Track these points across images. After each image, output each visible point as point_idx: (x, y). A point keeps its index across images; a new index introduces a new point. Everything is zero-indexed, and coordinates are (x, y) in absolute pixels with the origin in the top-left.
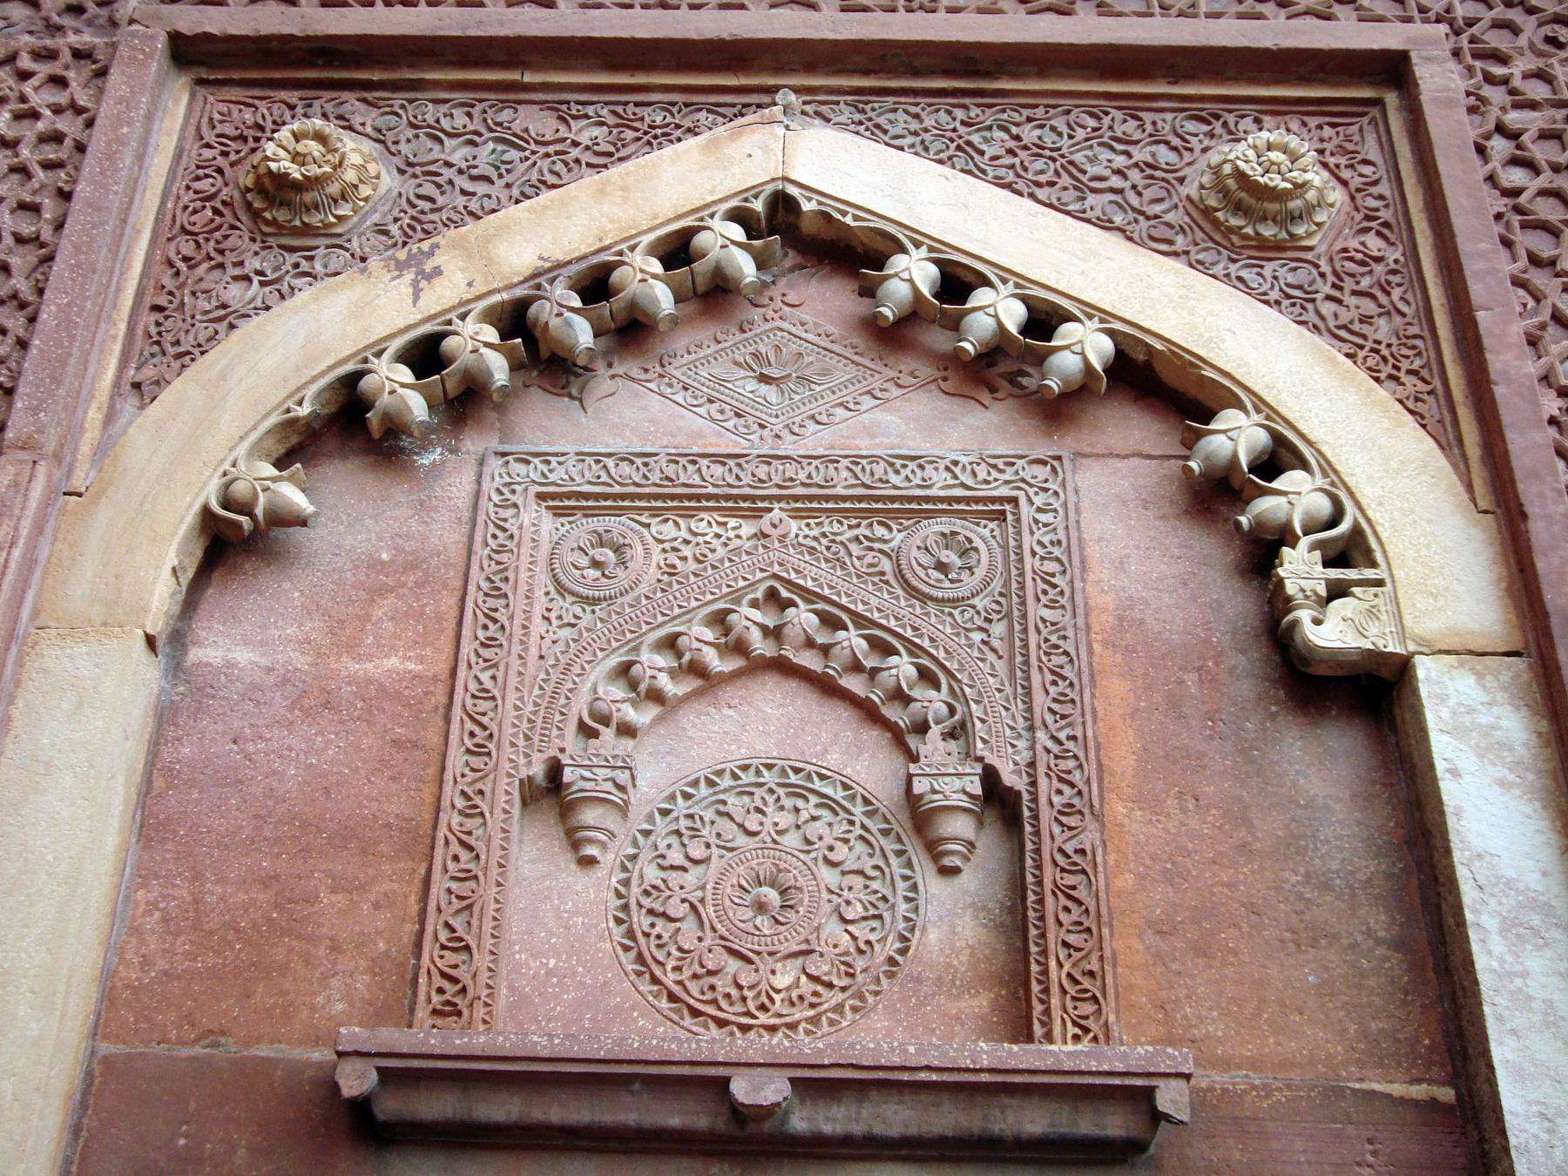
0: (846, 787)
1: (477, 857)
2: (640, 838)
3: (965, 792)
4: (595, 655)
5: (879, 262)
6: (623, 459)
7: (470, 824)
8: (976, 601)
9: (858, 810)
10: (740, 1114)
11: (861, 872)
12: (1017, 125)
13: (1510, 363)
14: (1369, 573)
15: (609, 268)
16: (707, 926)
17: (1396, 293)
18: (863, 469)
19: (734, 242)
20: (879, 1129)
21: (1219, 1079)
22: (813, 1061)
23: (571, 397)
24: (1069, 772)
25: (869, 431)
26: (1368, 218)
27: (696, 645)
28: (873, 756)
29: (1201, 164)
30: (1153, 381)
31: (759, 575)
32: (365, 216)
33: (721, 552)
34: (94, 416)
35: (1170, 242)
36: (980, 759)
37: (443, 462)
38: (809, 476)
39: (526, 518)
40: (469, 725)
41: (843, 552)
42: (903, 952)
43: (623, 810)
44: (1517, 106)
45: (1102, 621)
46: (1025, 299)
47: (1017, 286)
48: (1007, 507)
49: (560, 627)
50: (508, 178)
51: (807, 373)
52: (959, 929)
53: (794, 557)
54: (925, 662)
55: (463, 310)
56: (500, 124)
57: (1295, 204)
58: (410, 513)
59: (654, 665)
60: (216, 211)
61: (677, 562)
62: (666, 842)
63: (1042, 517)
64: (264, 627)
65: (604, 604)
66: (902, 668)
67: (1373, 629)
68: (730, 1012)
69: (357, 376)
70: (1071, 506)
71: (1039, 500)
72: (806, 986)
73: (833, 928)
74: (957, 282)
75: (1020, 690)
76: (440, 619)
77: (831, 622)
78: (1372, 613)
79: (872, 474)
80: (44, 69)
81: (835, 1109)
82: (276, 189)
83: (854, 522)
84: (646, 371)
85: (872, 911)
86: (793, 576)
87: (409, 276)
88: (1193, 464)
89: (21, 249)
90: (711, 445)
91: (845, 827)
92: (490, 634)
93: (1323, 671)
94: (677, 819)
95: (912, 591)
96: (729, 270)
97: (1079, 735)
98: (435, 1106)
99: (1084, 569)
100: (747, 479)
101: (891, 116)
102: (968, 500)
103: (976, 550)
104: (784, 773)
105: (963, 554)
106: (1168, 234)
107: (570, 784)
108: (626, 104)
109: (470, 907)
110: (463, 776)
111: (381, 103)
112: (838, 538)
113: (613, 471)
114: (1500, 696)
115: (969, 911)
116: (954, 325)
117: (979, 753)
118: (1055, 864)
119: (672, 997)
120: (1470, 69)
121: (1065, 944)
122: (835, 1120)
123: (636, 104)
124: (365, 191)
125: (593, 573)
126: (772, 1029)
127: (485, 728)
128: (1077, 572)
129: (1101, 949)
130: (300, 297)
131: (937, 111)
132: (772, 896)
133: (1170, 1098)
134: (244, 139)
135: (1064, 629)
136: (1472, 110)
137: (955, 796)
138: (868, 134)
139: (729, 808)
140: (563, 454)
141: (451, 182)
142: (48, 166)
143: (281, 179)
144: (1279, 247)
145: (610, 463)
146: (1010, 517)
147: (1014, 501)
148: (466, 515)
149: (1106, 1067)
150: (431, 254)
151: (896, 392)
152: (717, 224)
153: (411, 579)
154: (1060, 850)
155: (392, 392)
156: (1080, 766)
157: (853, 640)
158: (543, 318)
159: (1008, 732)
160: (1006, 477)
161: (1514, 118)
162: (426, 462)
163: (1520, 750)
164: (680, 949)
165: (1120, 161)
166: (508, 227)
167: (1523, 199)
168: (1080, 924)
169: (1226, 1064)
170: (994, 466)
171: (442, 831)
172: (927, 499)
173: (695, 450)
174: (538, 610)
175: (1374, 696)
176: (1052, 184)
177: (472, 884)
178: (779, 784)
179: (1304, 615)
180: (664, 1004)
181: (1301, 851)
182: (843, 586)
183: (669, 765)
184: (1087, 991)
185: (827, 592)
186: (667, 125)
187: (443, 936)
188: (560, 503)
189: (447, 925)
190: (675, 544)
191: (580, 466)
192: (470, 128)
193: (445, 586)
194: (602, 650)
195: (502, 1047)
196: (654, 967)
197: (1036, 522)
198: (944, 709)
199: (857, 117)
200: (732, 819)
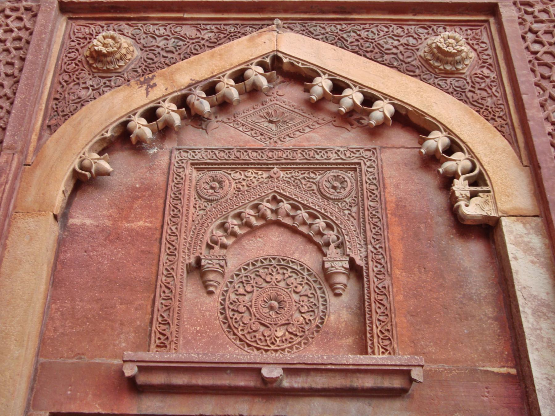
0: (301, 265)
1: (172, 291)
2: (228, 284)
3: (343, 267)
4: (212, 220)
5: (311, 80)
6: (221, 151)
7: (169, 280)
8: (346, 200)
9: (306, 273)
10: (265, 380)
11: (307, 296)
12: (359, 31)
13: (534, 113)
14: (485, 188)
15: (215, 83)
16: (253, 315)
17: (494, 89)
18: (306, 153)
19: (260, 74)
20: (314, 386)
21: (434, 367)
22: (290, 362)
23: (202, 129)
24: (380, 259)
25: (308, 140)
26: (484, 62)
27: (248, 216)
28: (311, 254)
29: (425, 44)
31: (270, 191)
32: (129, 65)
33: (256, 183)
34: (34, 137)
35: (414, 72)
36: (348, 255)
37: (158, 152)
38: (287, 156)
39: (187, 172)
40: (168, 245)
41: (299, 183)
42: (322, 323)
43: (223, 274)
44: (536, 22)
45: (391, 206)
46: (363, 93)
47: (360, 88)
48: (357, 166)
49: (200, 210)
50: (179, 52)
51: (286, 119)
52: (341, 315)
53: (282, 185)
54: (329, 221)
55: (164, 98)
56: (176, 32)
57: (458, 58)
58: (146, 170)
59: (233, 223)
60: (76, 64)
61: (241, 187)
62: (238, 286)
63: (370, 170)
64: (96, 211)
65: (215, 202)
66: (321, 223)
67: (486, 208)
68: (261, 345)
69: (127, 122)
70: (380, 166)
71: (368, 164)
72: (288, 336)
73: (297, 315)
74: (339, 87)
75: (362, 231)
76: (157, 208)
77: (295, 208)
78: (486, 202)
79: (309, 155)
80: (14, 15)
81: (298, 378)
82: (97, 56)
83: (303, 172)
84: (229, 119)
85: (311, 309)
86: (282, 191)
87: (145, 87)
88: (423, 151)
89: (8, 79)
90: (252, 145)
91: (301, 279)
92: (175, 213)
93: (469, 223)
94: (242, 277)
95: (324, 196)
96: (258, 83)
97: (383, 246)
98: (158, 379)
99: (384, 187)
100: (265, 157)
101: (315, 28)
102: (343, 164)
103: (346, 181)
104: (279, 261)
105: (342, 183)
106: (413, 69)
107: (204, 266)
108: (221, 24)
109: (169, 309)
110: (166, 263)
111: (134, 25)
112: (297, 178)
113: (218, 155)
114: (531, 231)
115: (345, 309)
116: (338, 102)
117: (348, 253)
118: (375, 292)
119: (241, 340)
120: (520, 9)
121: (379, 320)
122: (298, 383)
123: (225, 25)
124: (129, 57)
125: (211, 191)
126: (276, 351)
127: (173, 246)
128: (382, 189)
129: (391, 322)
130: (106, 95)
131: (331, 26)
132: (276, 304)
133: (416, 374)
134: (85, 38)
135: (377, 209)
136: (520, 24)
137: (339, 268)
138: (306, 34)
139: (260, 273)
140: (200, 149)
141: (159, 53)
142: (16, 49)
143: (99, 53)
144: (452, 73)
145: (217, 152)
146: (358, 170)
147: (359, 164)
148: (166, 171)
149: (394, 363)
150: (152, 79)
151: (317, 126)
152: (253, 67)
153: (147, 194)
154: (377, 287)
155: (139, 128)
156: (384, 257)
157: (303, 214)
158: (193, 101)
159: (358, 246)
160: (357, 155)
161: (535, 26)
162: (152, 152)
163: (539, 250)
164: (243, 323)
165: (396, 43)
166: (179, 69)
167: (538, 55)
168: (384, 313)
169: (436, 361)
170: (352, 152)
171: (159, 283)
172: (329, 164)
173: (247, 147)
174: (192, 204)
175: (487, 231)
176: (372, 51)
177: (170, 301)
178: (277, 265)
179: (462, 203)
180: (238, 342)
181: (461, 287)
182: (299, 195)
183: (239, 258)
184: (386, 336)
185: (294, 197)
186: (235, 32)
187: (160, 319)
188: (199, 166)
189: (161, 315)
190: (240, 180)
191: (206, 153)
192: (166, 34)
193: (159, 196)
194: (214, 218)
195: (181, 358)
196: (234, 329)
197: (367, 171)
198: (335, 238)
199: (303, 28)
200: (261, 277)
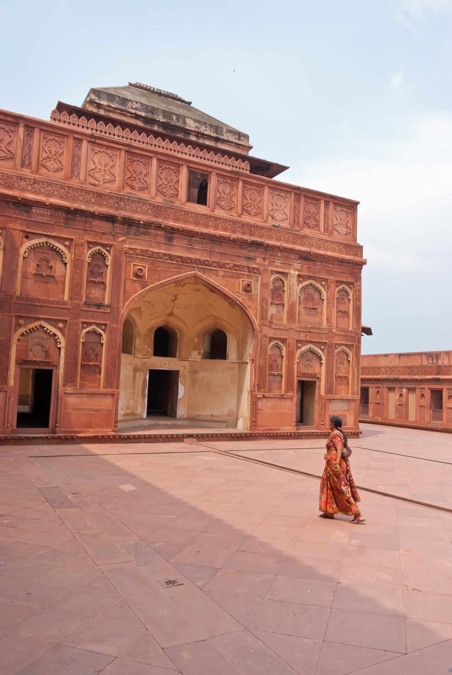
30: (55, 335)
74: (47, 329)
175: (60, 349)
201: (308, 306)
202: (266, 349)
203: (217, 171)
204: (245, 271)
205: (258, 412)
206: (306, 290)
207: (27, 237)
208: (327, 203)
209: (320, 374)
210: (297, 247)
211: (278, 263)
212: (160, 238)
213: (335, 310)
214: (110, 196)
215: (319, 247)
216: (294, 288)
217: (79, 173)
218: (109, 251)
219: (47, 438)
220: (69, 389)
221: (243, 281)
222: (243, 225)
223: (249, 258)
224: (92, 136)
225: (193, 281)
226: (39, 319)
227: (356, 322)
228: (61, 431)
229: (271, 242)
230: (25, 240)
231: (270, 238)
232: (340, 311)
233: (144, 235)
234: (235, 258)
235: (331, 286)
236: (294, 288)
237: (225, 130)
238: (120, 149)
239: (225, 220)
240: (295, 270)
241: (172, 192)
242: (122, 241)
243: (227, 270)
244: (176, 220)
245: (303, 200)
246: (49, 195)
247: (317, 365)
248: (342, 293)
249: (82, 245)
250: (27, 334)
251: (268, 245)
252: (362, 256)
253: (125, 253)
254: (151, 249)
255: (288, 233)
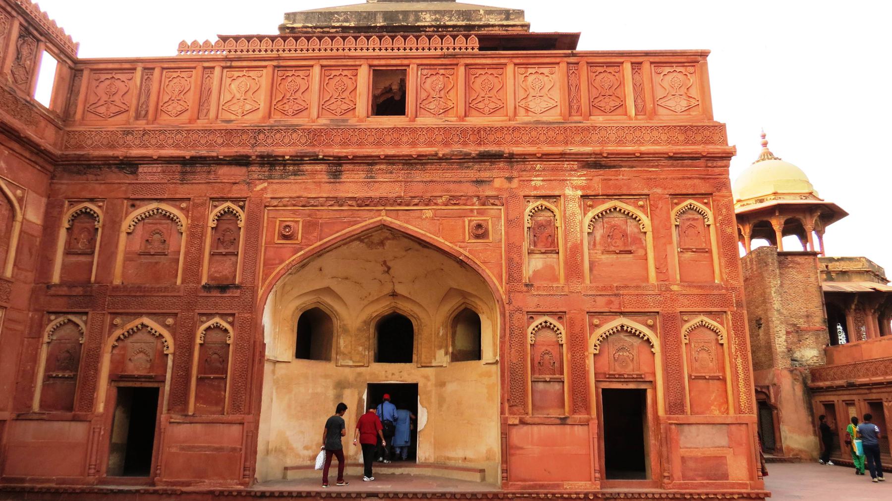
30: (161, 336)
201: (613, 248)
202: (524, 335)
203: (418, 61)
204: (473, 205)
205: (512, 451)
206: (605, 220)
207: (133, 206)
208: (637, 66)
209: (654, 374)
210: (575, 149)
211: (537, 181)
212: (320, 176)
213: (674, 250)
214: (244, 131)
215: (620, 142)
216: (575, 219)
217: (209, 110)
218: (242, 208)
219: (138, 491)
220: (177, 418)
221: (470, 221)
222: (464, 131)
223: (479, 182)
224: (226, 59)
225: (387, 234)
226: (141, 315)
227: (727, 267)
228: (161, 481)
229: (517, 150)
230: (130, 209)
231: (517, 143)
232: (688, 250)
233: (295, 175)
234: (451, 186)
235: (660, 206)
236: (575, 219)
237: (482, 12)
238: (265, 67)
239: (430, 130)
240: (576, 188)
241: (345, 107)
242: (262, 190)
243: (439, 207)
244: (344, 144)
245: (584, 69)
246: (162, 147)
247: (645, 356)
248: (690, 216)
249: (203, 204)
250: (125, 337)
251: (512, 156)
252: (725, 142)
253: (266, 206)
254: (305, 195)
255: (553, 129)
